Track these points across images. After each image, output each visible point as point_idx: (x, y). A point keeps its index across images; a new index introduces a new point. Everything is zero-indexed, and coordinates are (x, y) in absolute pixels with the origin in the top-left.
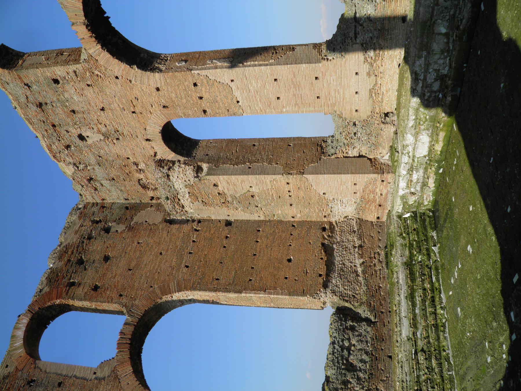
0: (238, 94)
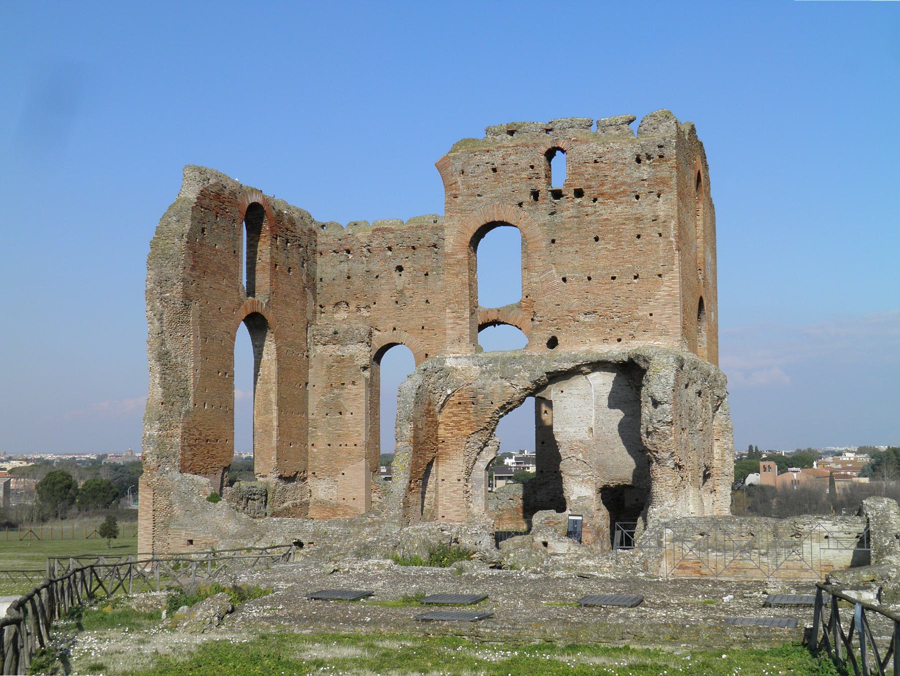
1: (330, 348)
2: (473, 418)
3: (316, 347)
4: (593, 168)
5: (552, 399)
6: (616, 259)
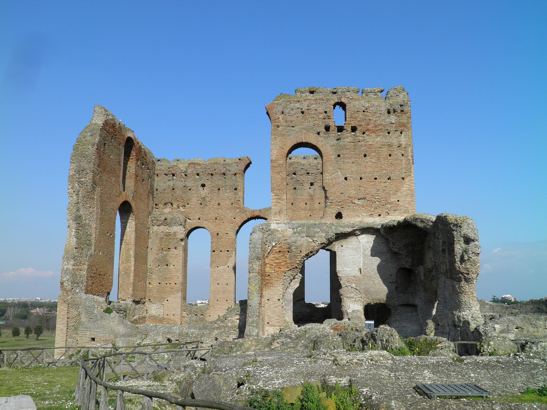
0: (221, 268)
1: (162, 228)
2: (288, 261)
4: (362, 114)
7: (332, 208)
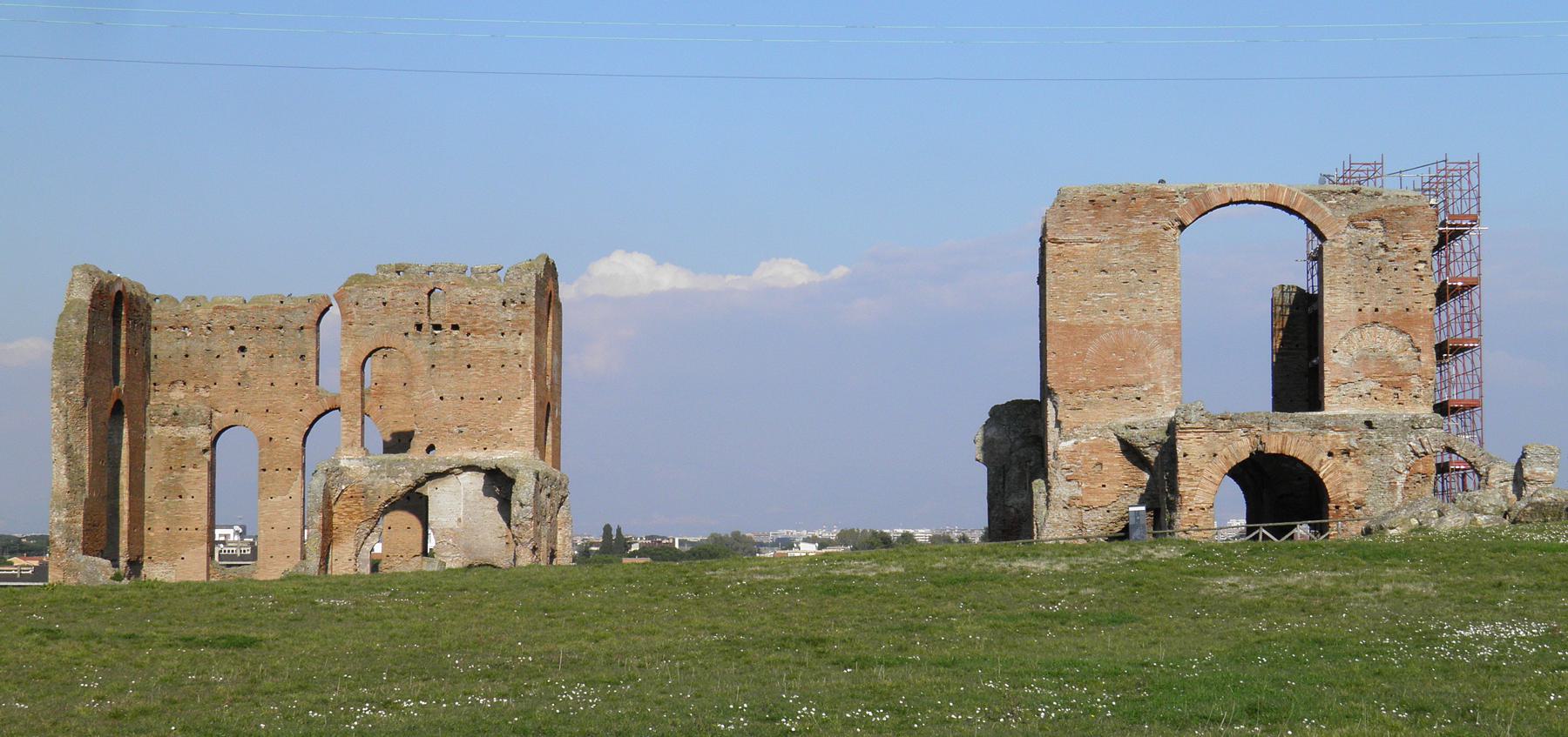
1: (169, 430)
2: (363, 509)
3: (153, 428)
4: (467, 308)
5: (428, 494)
6: (485, 383)
7: (422, 439)
